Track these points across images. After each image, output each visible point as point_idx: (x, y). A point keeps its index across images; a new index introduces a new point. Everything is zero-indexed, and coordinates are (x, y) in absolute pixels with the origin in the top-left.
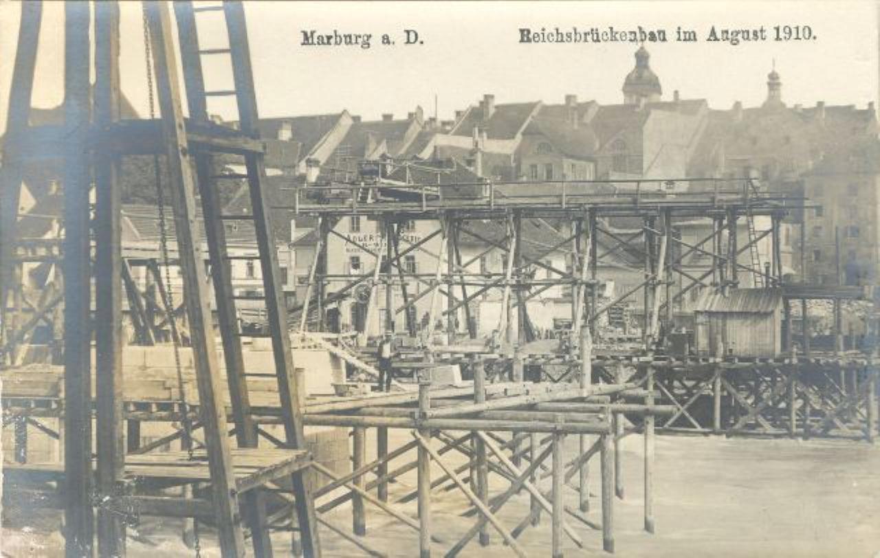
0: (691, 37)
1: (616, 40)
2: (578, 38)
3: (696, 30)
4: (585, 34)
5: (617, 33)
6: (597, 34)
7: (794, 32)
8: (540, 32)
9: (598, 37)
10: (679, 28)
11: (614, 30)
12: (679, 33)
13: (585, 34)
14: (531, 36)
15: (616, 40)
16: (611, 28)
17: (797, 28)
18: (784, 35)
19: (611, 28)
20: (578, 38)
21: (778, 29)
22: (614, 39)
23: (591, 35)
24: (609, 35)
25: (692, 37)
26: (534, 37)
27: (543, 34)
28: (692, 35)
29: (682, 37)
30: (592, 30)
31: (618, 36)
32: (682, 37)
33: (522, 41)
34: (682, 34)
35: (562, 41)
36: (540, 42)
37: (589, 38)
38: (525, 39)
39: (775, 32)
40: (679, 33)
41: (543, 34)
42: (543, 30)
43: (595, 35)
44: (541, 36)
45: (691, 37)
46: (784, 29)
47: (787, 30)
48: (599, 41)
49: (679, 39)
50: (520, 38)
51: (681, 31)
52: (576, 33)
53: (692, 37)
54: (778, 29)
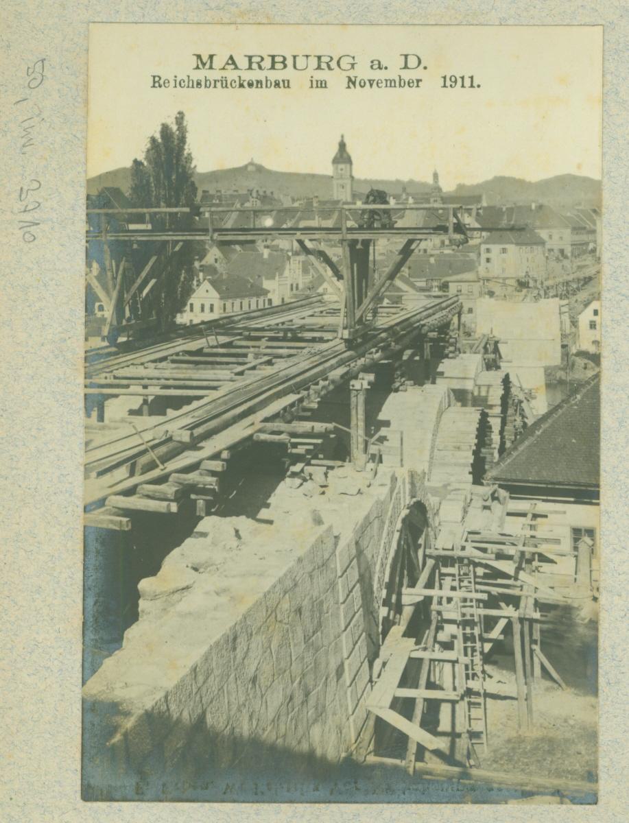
1: (244, 87)
2: (208, 85)
4: (215, 81)
7: (459, 81)
9: (226, 84)
11: (242, 79)
12: (312, 81)
13: (215, 81)
14: (162, 82)
15: (244, 87)
16: (240, 77)
17: (463, 78)
19: (240, 77)
20: (208, 85)
21: (445, 78)
22: (241, 86)
25: (323, 85)
26: (164, 83)
27: (176, 81)
29: (315, 85)
31: (245, 84)
32: (315, 85)
33: (154, 86)
36: (377, 79)
37: (219, 84)
38: (157, 85)
40: (312, 81)
43: (224, 82)
46: (450, 79)
47: (453, 79)
49: (312, 87)
51: (314, 80)
53: (323, 85)
54: (445, 78)
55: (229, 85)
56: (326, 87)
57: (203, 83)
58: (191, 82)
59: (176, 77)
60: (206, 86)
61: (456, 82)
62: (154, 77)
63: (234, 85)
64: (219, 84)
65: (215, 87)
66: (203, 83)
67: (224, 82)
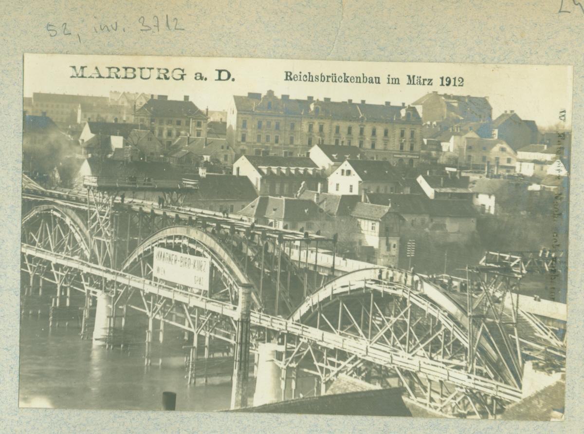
1: (348, 82)
5: (348, 77)
6: (336, 77)
11: (347, 75)
15: (348, 82)
22: (346, 81)
24: (343, 79)
31: (349, 79)
35: (312, 81)
37: (330, 79)
38: (289, 78)
43: (334, 78)
44: (299, 77)
48: (335, 81)
49: (389, 83)
55: (337, 80)
56: (398, 83)
57: (320, 78)
58: (311, 77)
60: (321, 80)
63: (340, 80)
64: (330, 79)
65: (328, 81)
67: (334, 78)
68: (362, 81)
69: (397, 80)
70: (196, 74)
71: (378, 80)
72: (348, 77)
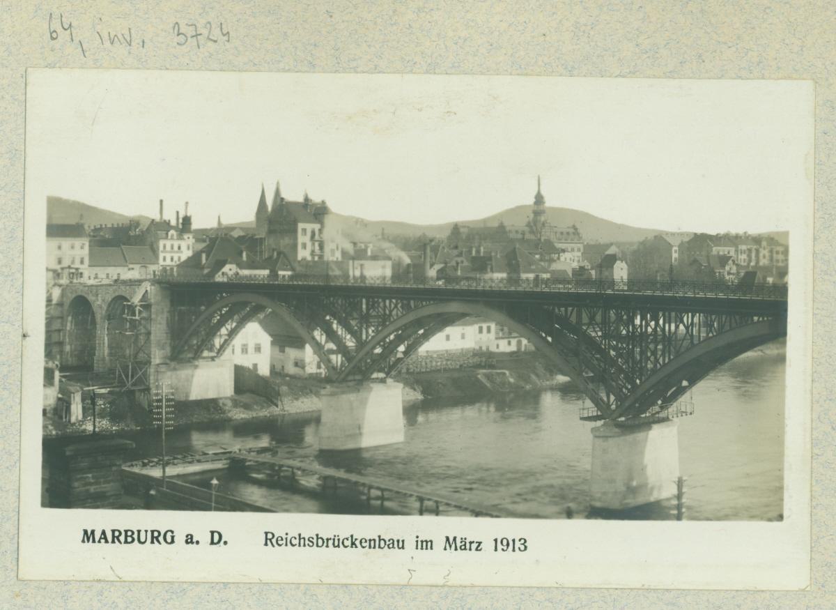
0: (426, 544)
3: (433, 539)
4: (328, 540)
5: (356, 539)
6: (339, 540)
8: (284, 537)
10: (417, 537)
11: (354, 538)
12: (417, 541)
15: (356, 547)
17: (514, 541)
18: (503, 547)
19: (352, 536)
21: (496, 540)
23: (332, 541)
28: (429, 544)
30: (335, 536)
31: (357, 543)
34: (420, 543)
37: (331, 542)
39: (494, 542)
40: (417, 541)
41: (286, 539)
42: (287, 534)
44: (285, 540)
45: (426, 544)
47: (505, 542)
48: (338, 546)
50: (264, 542)
51: (419, 539)
52: (318, 539)
59: (287, 534)
61: (508, 545)
62: (266, 533)
66: (315, 541)
68: (377, 546)
69: (429, 544)
70: (187, 536)
71: (401, 545)
72: (356, 539)
